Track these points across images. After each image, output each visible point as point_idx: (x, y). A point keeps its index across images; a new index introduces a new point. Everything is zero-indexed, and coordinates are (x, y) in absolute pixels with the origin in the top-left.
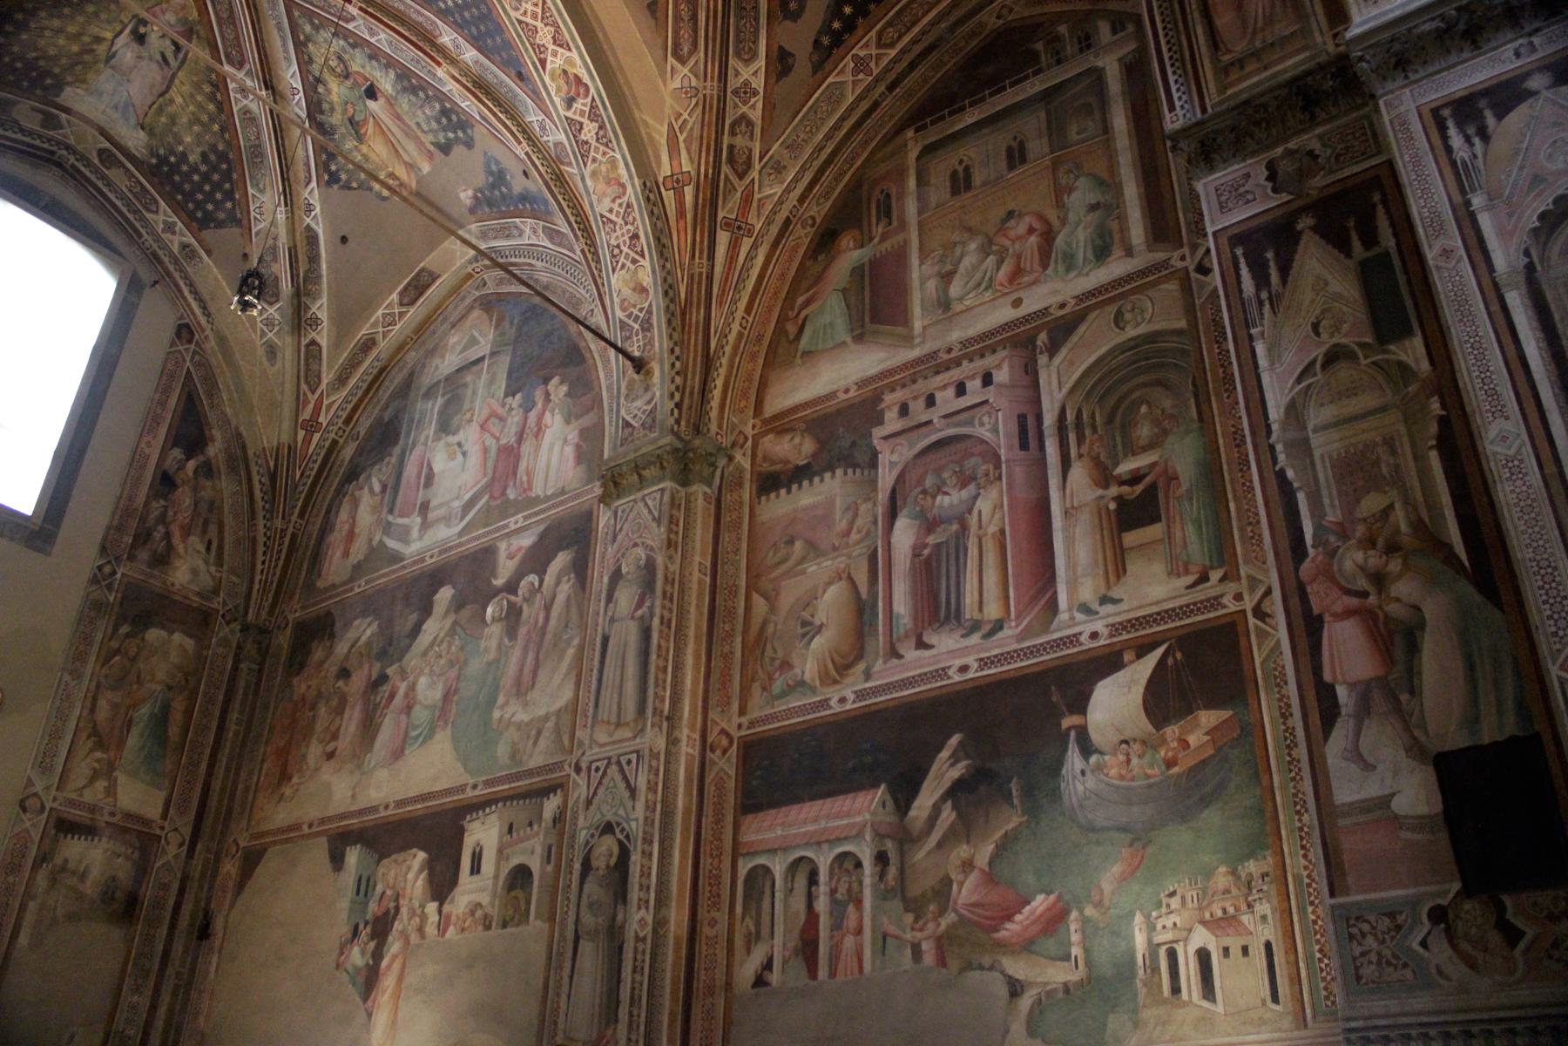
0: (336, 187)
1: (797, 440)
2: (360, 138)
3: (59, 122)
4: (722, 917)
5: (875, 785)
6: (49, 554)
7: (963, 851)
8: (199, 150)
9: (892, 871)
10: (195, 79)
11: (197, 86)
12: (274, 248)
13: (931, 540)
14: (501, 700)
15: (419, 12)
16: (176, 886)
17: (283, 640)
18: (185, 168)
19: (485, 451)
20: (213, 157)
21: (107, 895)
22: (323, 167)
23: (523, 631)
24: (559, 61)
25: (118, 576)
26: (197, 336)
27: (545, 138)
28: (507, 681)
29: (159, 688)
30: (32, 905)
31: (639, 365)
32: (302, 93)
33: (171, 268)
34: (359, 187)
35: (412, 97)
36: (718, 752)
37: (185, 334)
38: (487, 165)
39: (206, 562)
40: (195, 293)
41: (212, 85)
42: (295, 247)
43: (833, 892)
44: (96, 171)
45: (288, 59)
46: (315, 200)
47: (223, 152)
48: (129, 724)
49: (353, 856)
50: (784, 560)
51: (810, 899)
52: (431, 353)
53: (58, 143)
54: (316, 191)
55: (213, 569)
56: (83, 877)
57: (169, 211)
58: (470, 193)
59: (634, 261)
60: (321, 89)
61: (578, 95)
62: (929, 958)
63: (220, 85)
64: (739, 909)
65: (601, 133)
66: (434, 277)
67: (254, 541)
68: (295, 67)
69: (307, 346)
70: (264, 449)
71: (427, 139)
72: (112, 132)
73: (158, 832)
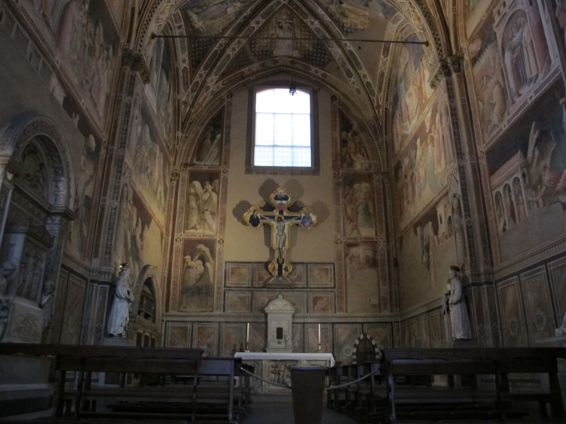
0: (349, 34)
1: (477, 42)
2: (346, 17)
4: (492, 212)
5: (517, 151)
6: (319, 175)
7: (543, 163)
9: (527, 178)
11: (301, 31)
12: (344, 61)
13: (515, 56)
14: (436, 167)
16: (386, 254)
17: (393, 173)
19: (415, 91)
21: (367, 260)
22: (343, 31)
23: (435, 143)
25: (340, 174)
26: (337, 97)
28: (436, 162)
29: (363, 200)
30: (348, 268)
31: (427, 44)
33: (322, 82)
36: (481, 159)
39: (364, 160)
40: (332, 86)
43: (515, 192)
45: (317, 8)
48: (357, 213)
49: (418, 229)
50: (483, 86)
51: (510, 197)
52: (398, 68)
55: (367, 161)
56: (359, 257)
57: (314, 67)
58: (382, 14)
59: (414, 11)
60: (329, 10)
62: (541, 205)
63: (306, 26)
64: (495, 208)
67: (376, 148)
68: (320, 9)
69: (366, 84)
70: (369, 121)
71: (361, 6)
73: (376, 240)
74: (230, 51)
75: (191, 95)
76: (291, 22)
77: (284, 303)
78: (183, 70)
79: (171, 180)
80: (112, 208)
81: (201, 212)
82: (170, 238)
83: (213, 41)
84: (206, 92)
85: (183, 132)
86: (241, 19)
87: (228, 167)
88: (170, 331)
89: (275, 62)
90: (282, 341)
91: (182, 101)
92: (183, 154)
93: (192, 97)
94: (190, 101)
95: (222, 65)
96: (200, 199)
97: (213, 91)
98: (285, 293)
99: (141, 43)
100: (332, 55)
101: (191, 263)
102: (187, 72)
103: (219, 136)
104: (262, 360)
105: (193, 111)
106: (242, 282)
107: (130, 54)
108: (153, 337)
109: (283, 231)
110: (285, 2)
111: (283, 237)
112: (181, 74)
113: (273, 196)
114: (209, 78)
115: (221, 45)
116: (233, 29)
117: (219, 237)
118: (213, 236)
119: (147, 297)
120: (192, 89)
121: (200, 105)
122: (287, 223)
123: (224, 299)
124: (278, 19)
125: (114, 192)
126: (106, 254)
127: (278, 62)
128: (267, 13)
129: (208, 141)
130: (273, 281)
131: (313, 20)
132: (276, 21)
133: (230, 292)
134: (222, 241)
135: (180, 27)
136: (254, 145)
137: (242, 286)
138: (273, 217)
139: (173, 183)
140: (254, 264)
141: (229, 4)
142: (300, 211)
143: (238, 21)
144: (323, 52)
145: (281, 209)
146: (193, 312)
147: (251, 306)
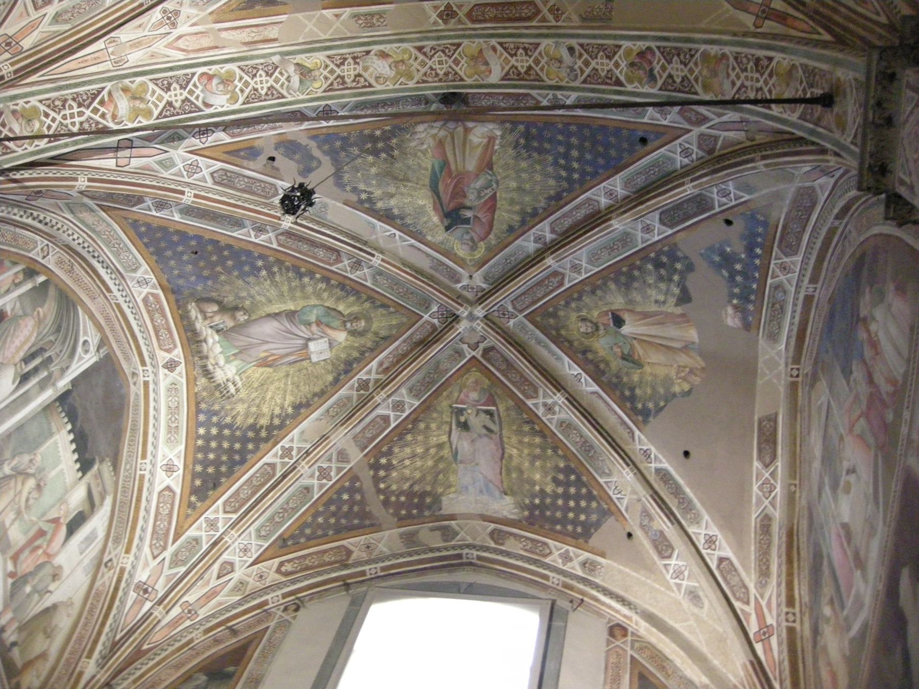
0: (651, 419)
2: (639, 364)
3: (453, 530)
8: (549, 478)
10: (514, 428)
11: (519, 432)
15: (577, 207)
18: (548, 501)
20: (561, 477)
24: (623, 64)
26: (630, 629)
27: (694, 156)
32: (584, 374)
34: (667, 401)
35: (636, 285)
37: (617, 632)
38: (712, 262)
41: (527, 422)
42: (656, 492)
44: (495, 551)
45: (559, 359)
46: (648, 446)
47: (565, 466)
54: (643, 437)
58: (730, 310)
59: (771, 75)
60: (590, 356)
61: (651, 63)
63: (532, 419)
65: (682, 57)
66: (773, 419)
69: (718, 567)
72: (489, 513)
74: (312, 476)
75: (167, 572)
76: (494, 408)
83: (263, 434)
84: (219, 577)
86: (352, 388)
89: (448, 534)
91: (136, 581)
94: (161, 588)
95: (286, 511)
97: (242, 584)
100: (610, 498)
102: (172, 505)
105: (156, 613)
110: (474, 353)
112: (151, 501)
114: (233, 532)
115: (287, 452)
120: (176, 554)
121: (190, 612)
128: (426, 383)
131: (550, 401)
132: (451, 406)
135: (171, 366)
141: (314, 328)
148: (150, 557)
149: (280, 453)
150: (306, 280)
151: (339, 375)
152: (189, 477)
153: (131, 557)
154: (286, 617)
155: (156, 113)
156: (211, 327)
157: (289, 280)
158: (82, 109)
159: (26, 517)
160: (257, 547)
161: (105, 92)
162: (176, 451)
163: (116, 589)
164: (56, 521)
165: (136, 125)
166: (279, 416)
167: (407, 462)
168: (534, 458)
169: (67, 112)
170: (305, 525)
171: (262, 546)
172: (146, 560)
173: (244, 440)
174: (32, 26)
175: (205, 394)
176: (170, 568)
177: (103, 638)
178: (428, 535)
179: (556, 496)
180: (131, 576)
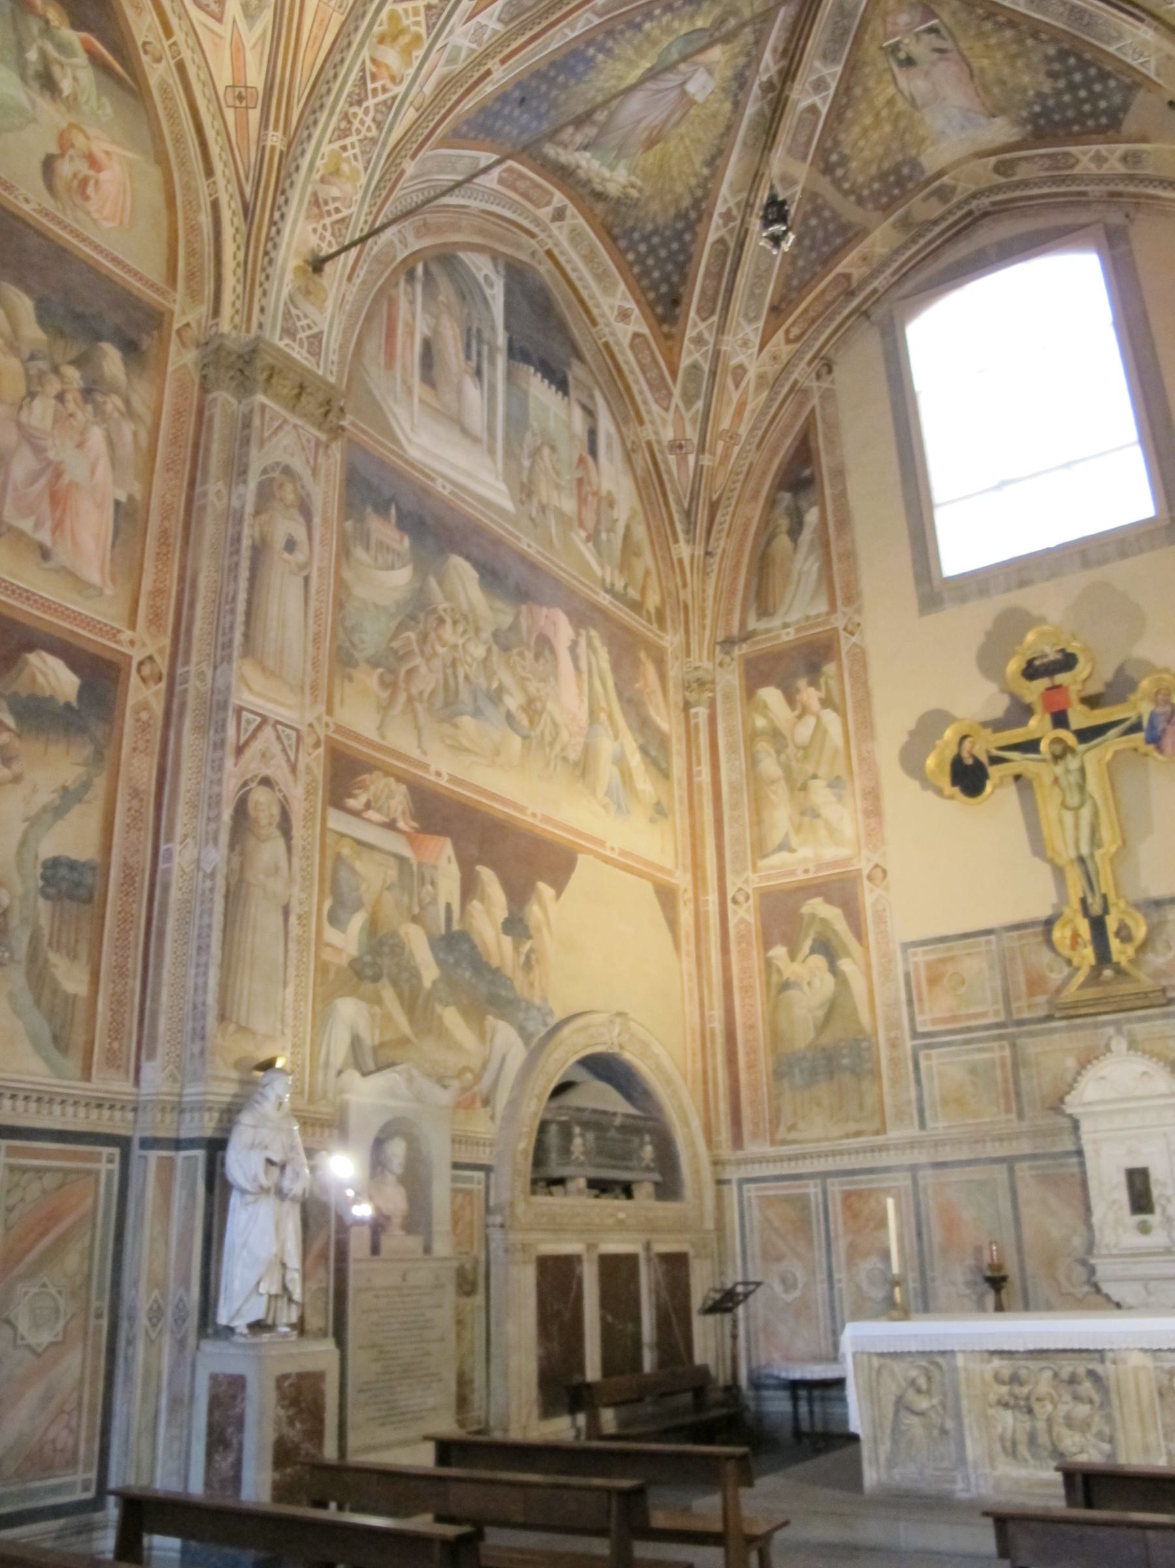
8: (1041, 77)
10: (972, 33)
11: (981, 35)
18: (1051, 102)
20: (1057, 66)
33: (1131, 189)
53: (966, 201)
75: (687, 416)
76: (935, 22)
77: (1141, 1068)
78: (632, 346)
79: (687, 706)
80: (205, 876)
81: (799, 787)
82: (713, 898)
83: (693, 215)
84: (737, 386)
85: (691, 541)
87: (859, 611)
88: (756, 1213)
89: (943, 194)
90: (1154, 1219)
92: (709, 612)
93: (693, 421)
94: (692, 434)
95: (760, 278)
96: (786, 746)
97: (761, 377)
98: (1139, 1029)
99: (264, 302)
100: (1130, 67)
101: (790, 970)
102: (649, 348)
103: (812, 517)
104: (952, 1353)
106: (973, 1010)
107: (219, 348)
108: (661, 1247)
109: (1082, 787)
111: (1086, 813)
112: (628, 359)
113: (1014, 666)
115: (727, 216)
116: (745, 143)
117: (869, 860)
118: (848, 860)
119: (586, 1125)
121: (733, 436)
122: (1095, 757)
123: (918, 1081)
124: (886, 38)
125: (209, 819)
126: (193, 1041)
127: (953, 189)
128: (838, 37)
129: (783, 541)
130: (1082, 986)
133: (934, 1052)
134: (880, 873)
135: (559, 215)
136: (930, 506)
137: (973, 1023)
138: (1030, 746)
139: (696, 715)
140: (1006, 935)
142: (1132, 698)
143: (750, 110)
144: (1093, 71)
145: (1056, 709)
146: (818, 1140)
147: (1018, 1095)
148: (662, 412)
149: (720, 222)
150: (647, 26)
151: (736, 95)
152: (648, 311)
153: (648, 426)
154: (825, 384)
155: (423, 31)
156: (577, 150)
157: (629, 41)
158: (365, 105)
159: (563, 483)
160: (752, 332)
161: (369, 65)
162: (619, 295)
163: (655, 463)
164: (581, 460)
165: (416, 64)
166: (698, 186)
167: (862, 143)
168: (1013, 58)
169: (356, 124)
170: (789, 278)
171: (757, 329)
172: (661, 417)
173: (679, 236)
174: (238, 51)
175: (610, 218)
176: (688, 410)
177: (676, 517)
178: (922, 208)
179: (1058, 93)
180: (659, 442)
